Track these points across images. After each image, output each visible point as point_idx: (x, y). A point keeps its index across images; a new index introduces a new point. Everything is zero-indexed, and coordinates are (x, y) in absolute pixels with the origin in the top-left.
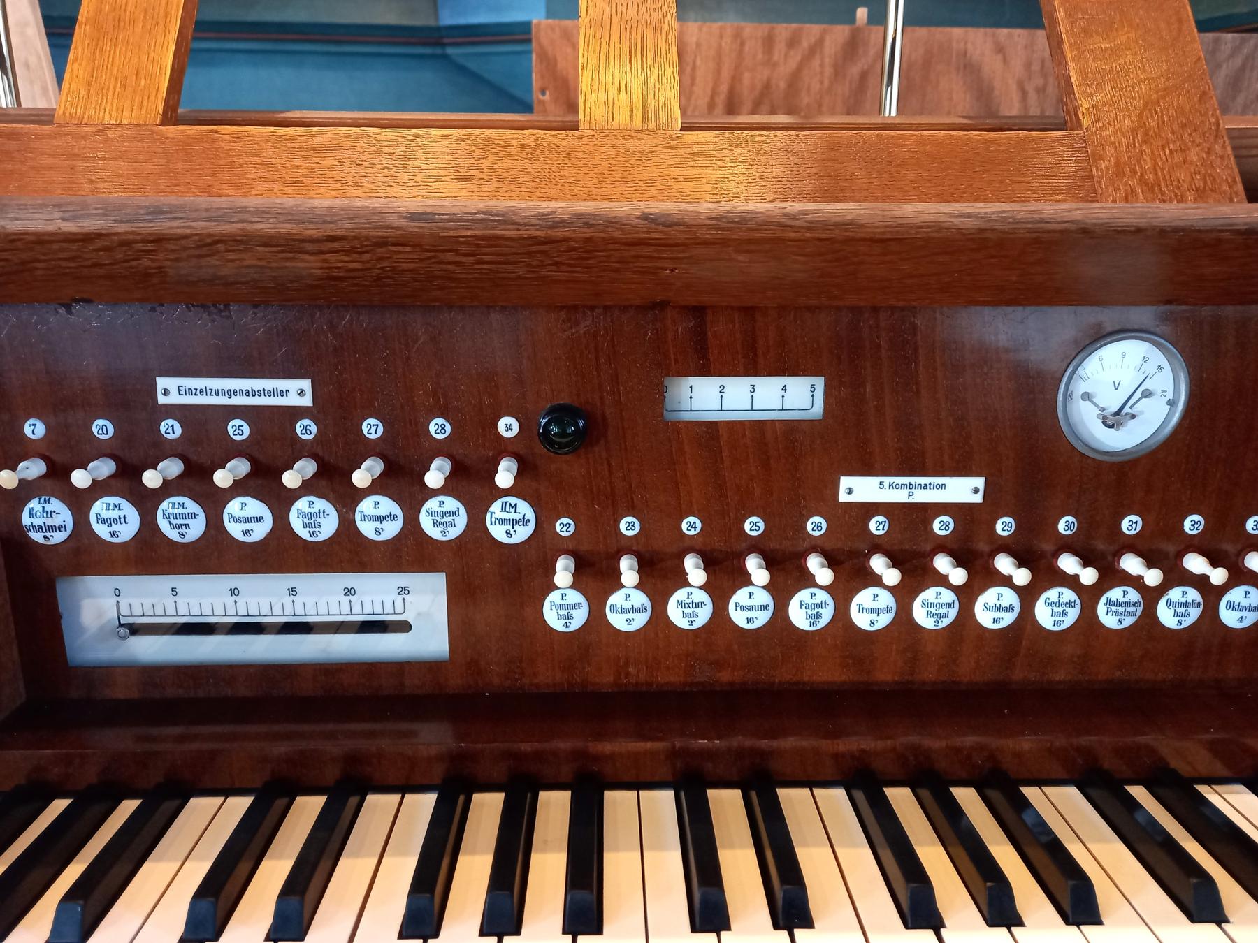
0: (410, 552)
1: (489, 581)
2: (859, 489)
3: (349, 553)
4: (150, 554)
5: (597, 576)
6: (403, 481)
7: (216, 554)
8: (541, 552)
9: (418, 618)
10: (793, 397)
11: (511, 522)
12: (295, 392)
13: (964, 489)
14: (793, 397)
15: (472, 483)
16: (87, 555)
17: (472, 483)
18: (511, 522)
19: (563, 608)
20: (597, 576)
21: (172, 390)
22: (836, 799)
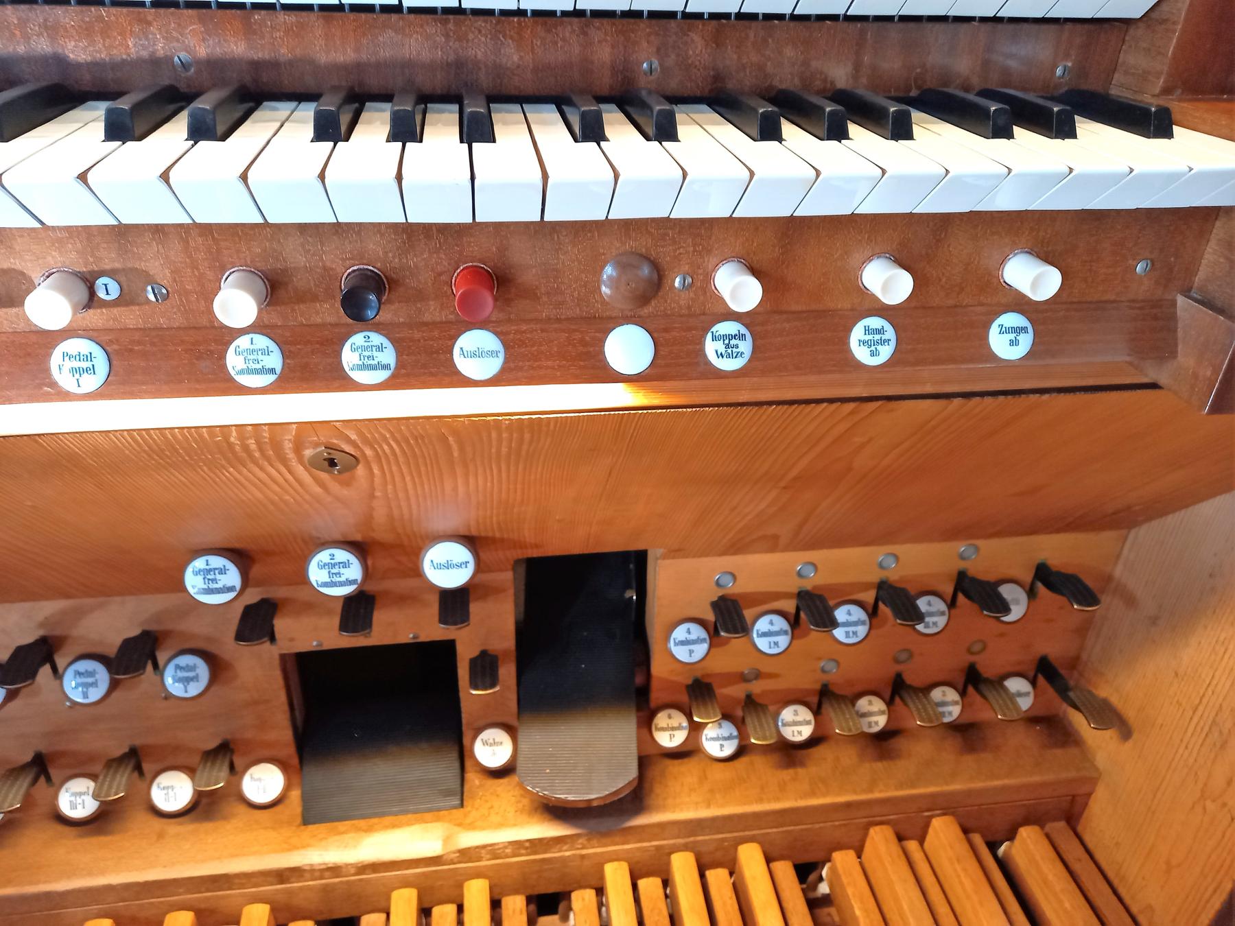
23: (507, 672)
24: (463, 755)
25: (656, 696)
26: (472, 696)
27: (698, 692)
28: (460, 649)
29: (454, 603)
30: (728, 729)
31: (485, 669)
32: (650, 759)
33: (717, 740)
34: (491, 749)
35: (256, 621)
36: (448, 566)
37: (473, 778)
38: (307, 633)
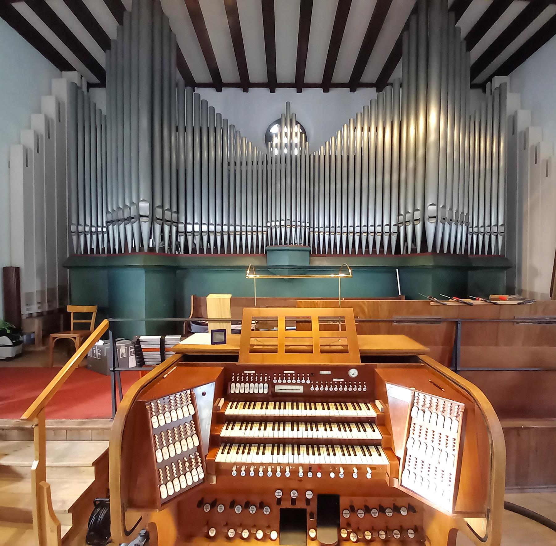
0: (301, 384)
1: (306, 386)
2: (334, 380)
3: (296, 384)
4: (282, 384)
5: (315, 387)
6: (301, 379)
7: (287, 384)
8: (310, 384)
9: (300, 389)
10: (329, 373)
11: (308, 382)
12: (293, 372)
13: (342, 380)
14: (329, 373)
15: (306, 379)
16: (278, 384)
17: (306, 379)
18: (308, 382)
19: (312, 389)
20: (315, 387)
21: (285, 372)
22: (333, 404)
23: (316, 516)
24: (307, 534)
25: (341, 526)
26: (310, 521)
27: (348, 525)
28: (308, 510)
29: (308, 501)
30: (355, 535)
31: (312, 516)
32: (340, 539)
33: (353, 538)
34: (312, 533)
35: (279, 501)
36: (309, 495)
37: (309, 540)
38: (287, 505)
